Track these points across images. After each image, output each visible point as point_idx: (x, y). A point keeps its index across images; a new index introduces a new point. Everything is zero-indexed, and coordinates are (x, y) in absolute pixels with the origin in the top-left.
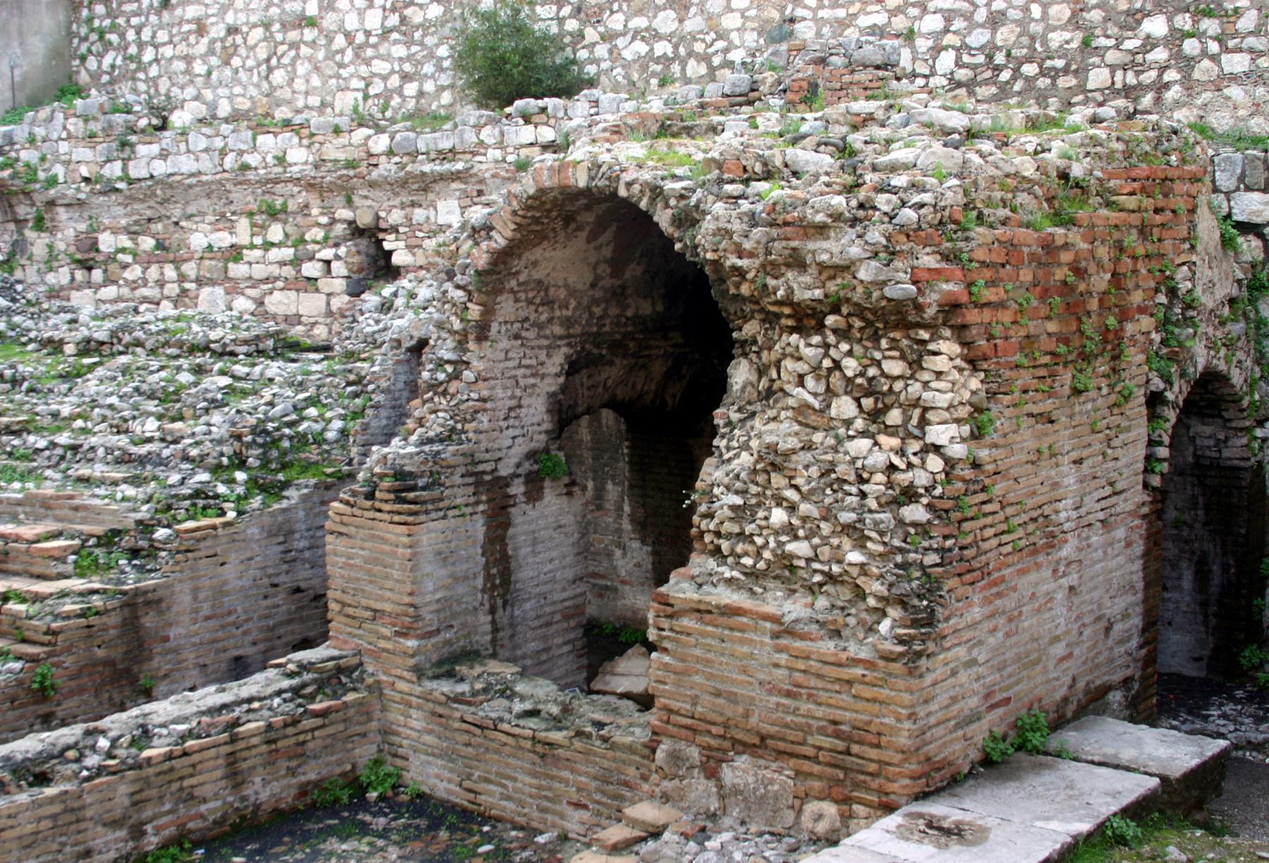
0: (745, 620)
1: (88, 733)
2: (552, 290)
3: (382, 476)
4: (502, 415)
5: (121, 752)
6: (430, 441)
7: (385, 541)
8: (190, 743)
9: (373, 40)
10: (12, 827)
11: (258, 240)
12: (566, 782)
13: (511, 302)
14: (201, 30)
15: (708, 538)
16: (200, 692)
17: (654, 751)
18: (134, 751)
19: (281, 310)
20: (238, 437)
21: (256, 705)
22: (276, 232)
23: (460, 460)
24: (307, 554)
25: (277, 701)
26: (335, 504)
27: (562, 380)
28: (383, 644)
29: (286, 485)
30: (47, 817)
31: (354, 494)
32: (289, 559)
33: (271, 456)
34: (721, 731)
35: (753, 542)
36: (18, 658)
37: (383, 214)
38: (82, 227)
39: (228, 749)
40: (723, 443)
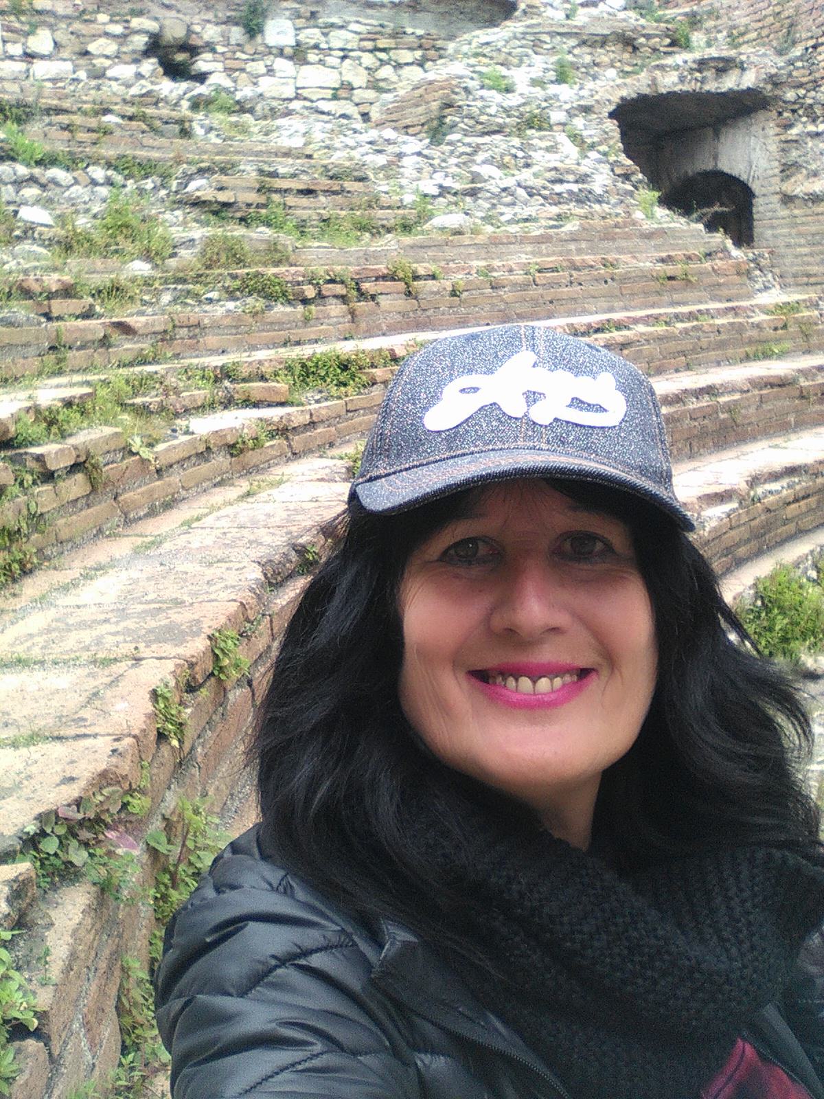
37: (197, 28)
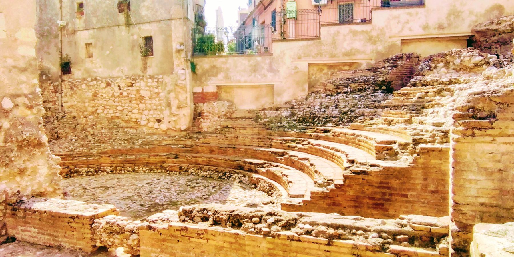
5: (274, 228)
10: (213, 240)
21: (359, 232)
30: (228, 242)
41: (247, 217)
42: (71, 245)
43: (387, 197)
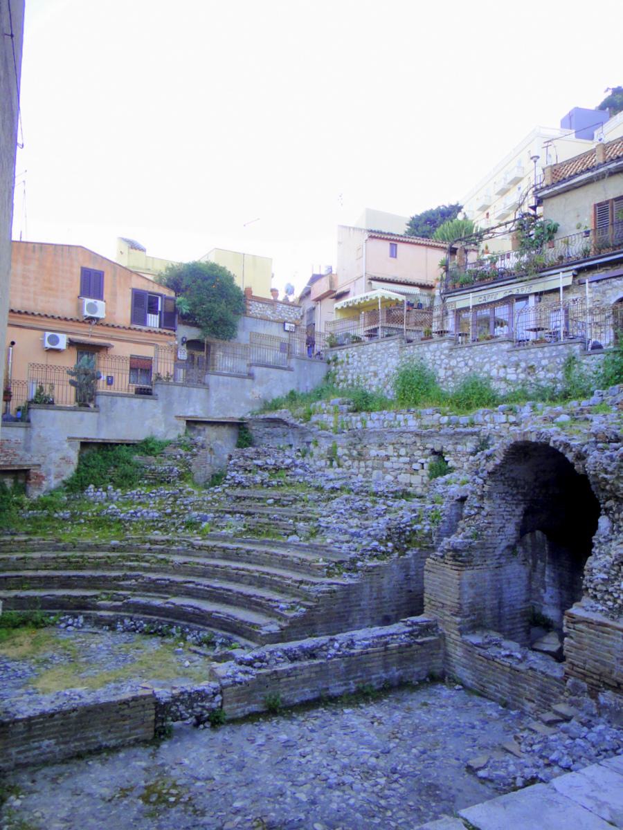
0: (609, 629)
1: (331, 640)
2: (518, 482)
3: (449, 550)
4: (497, 530)
6: (467, 538)
7: (449, 576)
8: (370, 649)
9: (441, 380)
11: (396, 454)
12: (525, 689)
13: (501, 485)
14: (376, 374)
15: (590, 591)
16: (374, 629)
17: (566, 681)
18: (348, 650)
19: (404, 481)
20: (390, 529)
21: (395, 637)
22: (403, 451)
23: (479, 546)
24: (415, 577)
25: (403, 636)
26: (428, 559)
27: (522, 518)
28: (446, 618)
29: (407, 549)
31: (436, 555)
32: (408, 578)
33: (402, 537)
34: (598, 678)
35: (612, 595)
36: (304, 606)
38: (330, 445)
39: (382, 653)
40: (597, 551)
41: (317, 648)
42: (120, 741)
43: (347, 609)
